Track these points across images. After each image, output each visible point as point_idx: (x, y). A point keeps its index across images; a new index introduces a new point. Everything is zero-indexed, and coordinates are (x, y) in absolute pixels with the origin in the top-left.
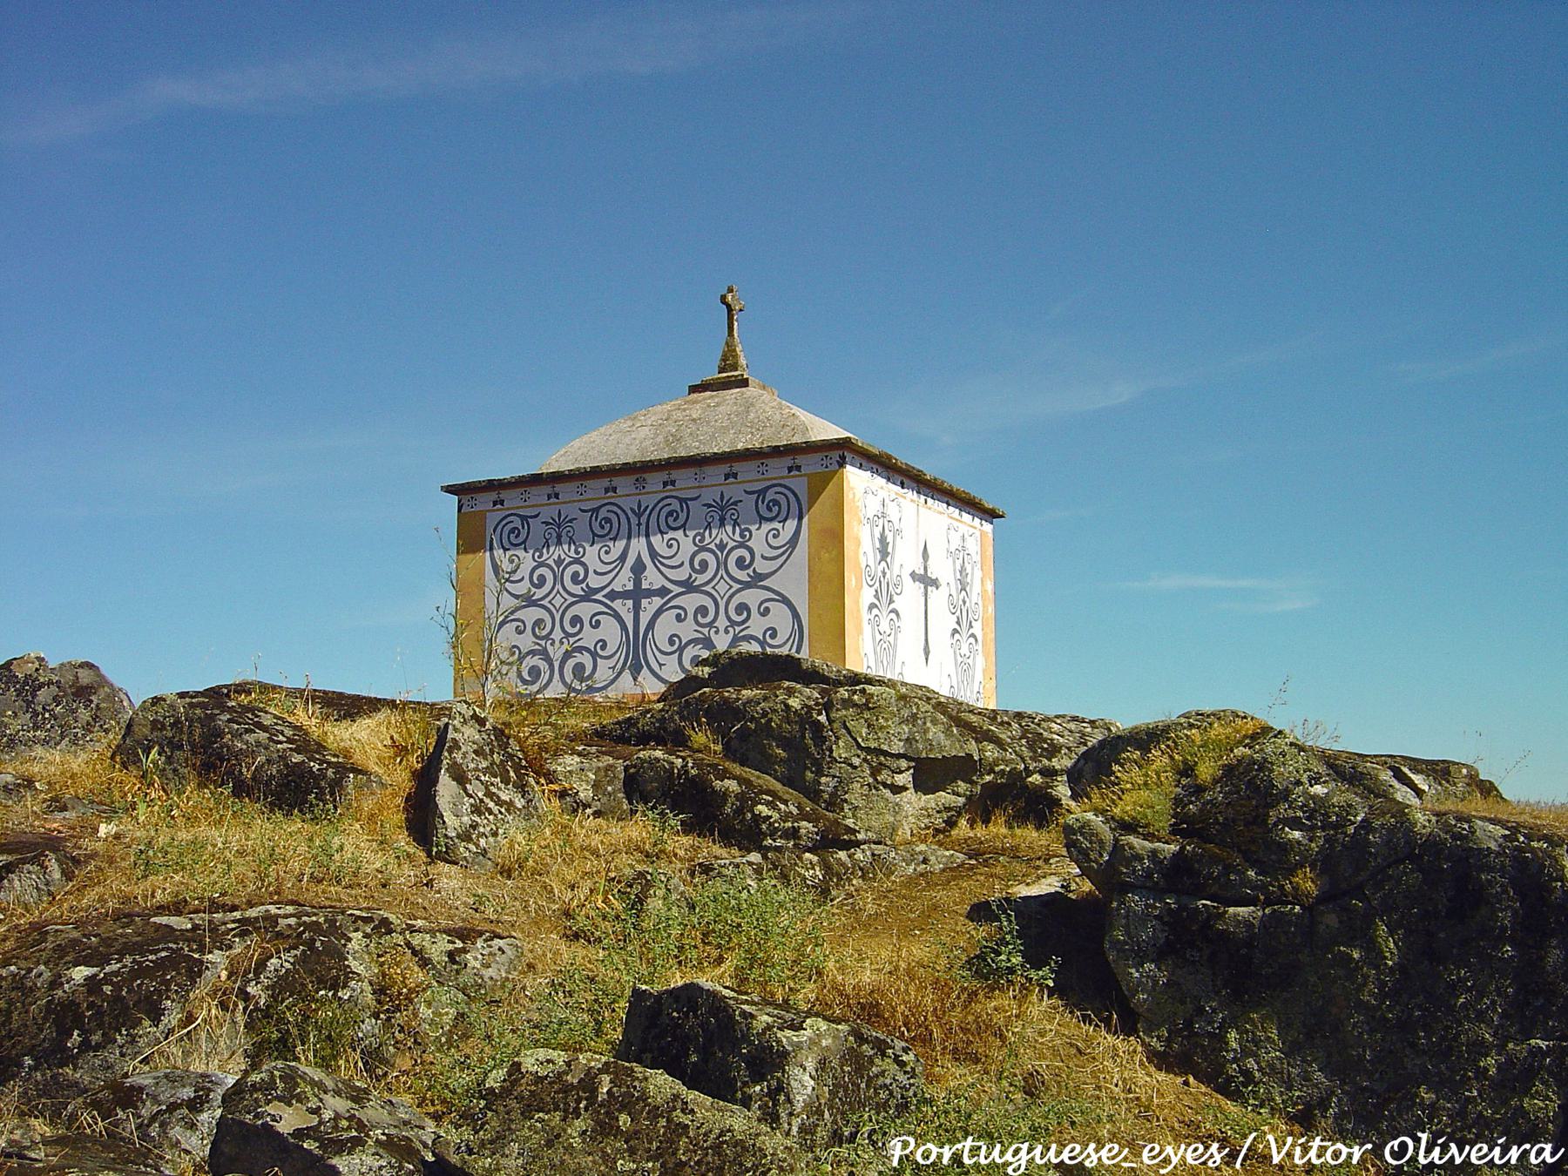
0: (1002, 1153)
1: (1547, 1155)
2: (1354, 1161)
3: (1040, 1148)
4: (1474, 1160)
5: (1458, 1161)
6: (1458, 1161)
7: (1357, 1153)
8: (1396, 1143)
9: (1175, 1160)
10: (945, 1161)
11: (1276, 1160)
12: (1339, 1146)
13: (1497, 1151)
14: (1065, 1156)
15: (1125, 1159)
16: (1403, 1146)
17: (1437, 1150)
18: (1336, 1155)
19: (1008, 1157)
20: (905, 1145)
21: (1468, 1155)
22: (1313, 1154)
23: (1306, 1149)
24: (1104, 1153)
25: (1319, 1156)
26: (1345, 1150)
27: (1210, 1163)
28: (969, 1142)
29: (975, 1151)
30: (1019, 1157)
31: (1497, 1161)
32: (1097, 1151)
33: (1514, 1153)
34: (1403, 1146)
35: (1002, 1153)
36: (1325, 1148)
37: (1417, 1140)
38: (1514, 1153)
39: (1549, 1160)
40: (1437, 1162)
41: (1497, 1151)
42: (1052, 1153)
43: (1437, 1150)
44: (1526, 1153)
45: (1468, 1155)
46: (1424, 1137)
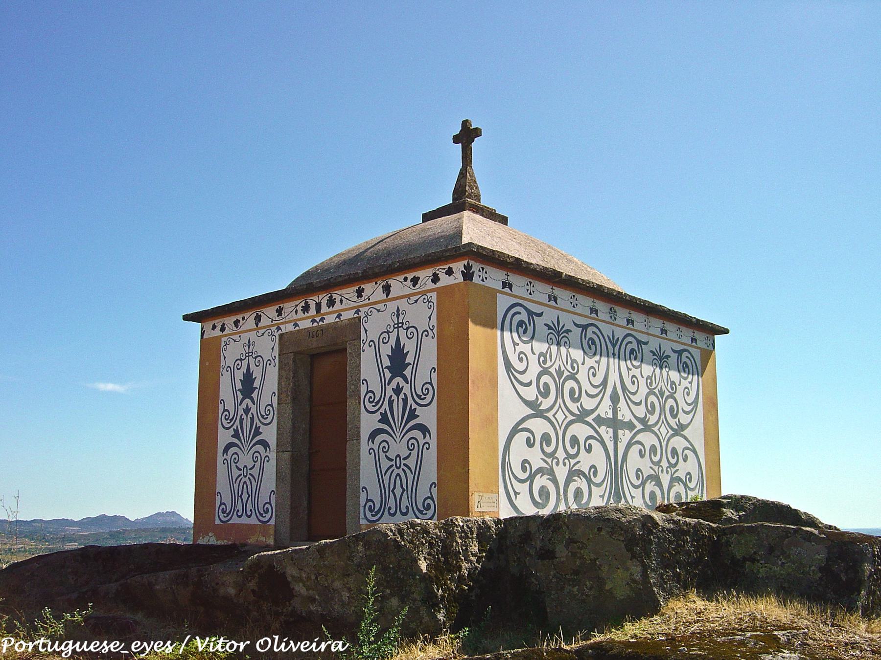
0: (59, 646)
1: (340, 646)
2: (241, 650)
3: (79, 643)
4: (112, 650)
5: (294, 650)
6: (294, 650)
7: (242, 646)
8: (262, 641)
9: (148, 650)
10: (30, 650)
11: (200, 649)
12: (233, 642)
13: (314, 645)
14: (92, 647)
15: (122, 649)
16: (266, 642)
17: (283, 644)
18: (231, 647)
19: (62, 647)
20: (9, 641)
21: (153, 648)
22: (219, 647)
23: (337, 645)
24: (112, 646)
25: (222, 648)
26: (236, 644)
27: (167, 651)
28: (42, 640)
29: (45, 646)
30: (69, 648)
31: (314, 650)
32: (108, 645)
33: (323, 646)
34: (266, 642)
35: (59, 646)
36: (226, 643)
37: (273, 640)
38: (323, 646)
39: (341, 650)
40: (283, 650)
41: (314, 645)
42: (85, 646)
43: (283, 644)
44: (329, 646)
45: (153, 648)
46: (277, 637)
